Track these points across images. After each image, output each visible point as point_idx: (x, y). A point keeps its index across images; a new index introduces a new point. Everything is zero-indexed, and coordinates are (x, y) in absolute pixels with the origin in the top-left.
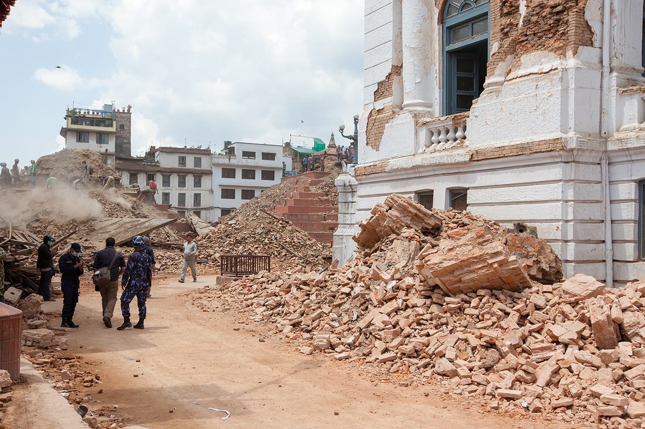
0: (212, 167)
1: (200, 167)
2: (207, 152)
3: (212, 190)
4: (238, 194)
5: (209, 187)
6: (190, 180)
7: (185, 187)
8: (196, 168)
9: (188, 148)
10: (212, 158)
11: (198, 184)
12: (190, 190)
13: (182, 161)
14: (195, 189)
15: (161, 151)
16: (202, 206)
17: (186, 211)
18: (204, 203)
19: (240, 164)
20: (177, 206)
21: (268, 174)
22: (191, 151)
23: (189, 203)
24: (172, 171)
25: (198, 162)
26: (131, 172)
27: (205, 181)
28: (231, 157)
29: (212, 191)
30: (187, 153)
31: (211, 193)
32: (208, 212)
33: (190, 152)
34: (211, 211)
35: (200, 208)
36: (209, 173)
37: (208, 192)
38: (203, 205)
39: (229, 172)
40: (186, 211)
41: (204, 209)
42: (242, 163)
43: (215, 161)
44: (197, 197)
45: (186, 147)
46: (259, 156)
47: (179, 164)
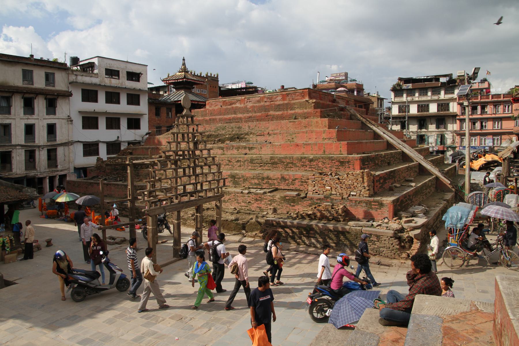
0: (68, 87)
1: (54, 86)
6: (40, 105)
9: (35, 57)
13: (27, 76)
14: (47, 117)
17: (37, 150)
18: (61, 136)
20: (23, 143)
22: (42, 63)
25: (49, 79)
30: (34, 65)
31: (70, 123)
32: (66, 148)
34: (71, 147)
37: (65, 121)
44: (51, 129)
45: (32, 56)
46: (123, 75)
47: (23, 81)
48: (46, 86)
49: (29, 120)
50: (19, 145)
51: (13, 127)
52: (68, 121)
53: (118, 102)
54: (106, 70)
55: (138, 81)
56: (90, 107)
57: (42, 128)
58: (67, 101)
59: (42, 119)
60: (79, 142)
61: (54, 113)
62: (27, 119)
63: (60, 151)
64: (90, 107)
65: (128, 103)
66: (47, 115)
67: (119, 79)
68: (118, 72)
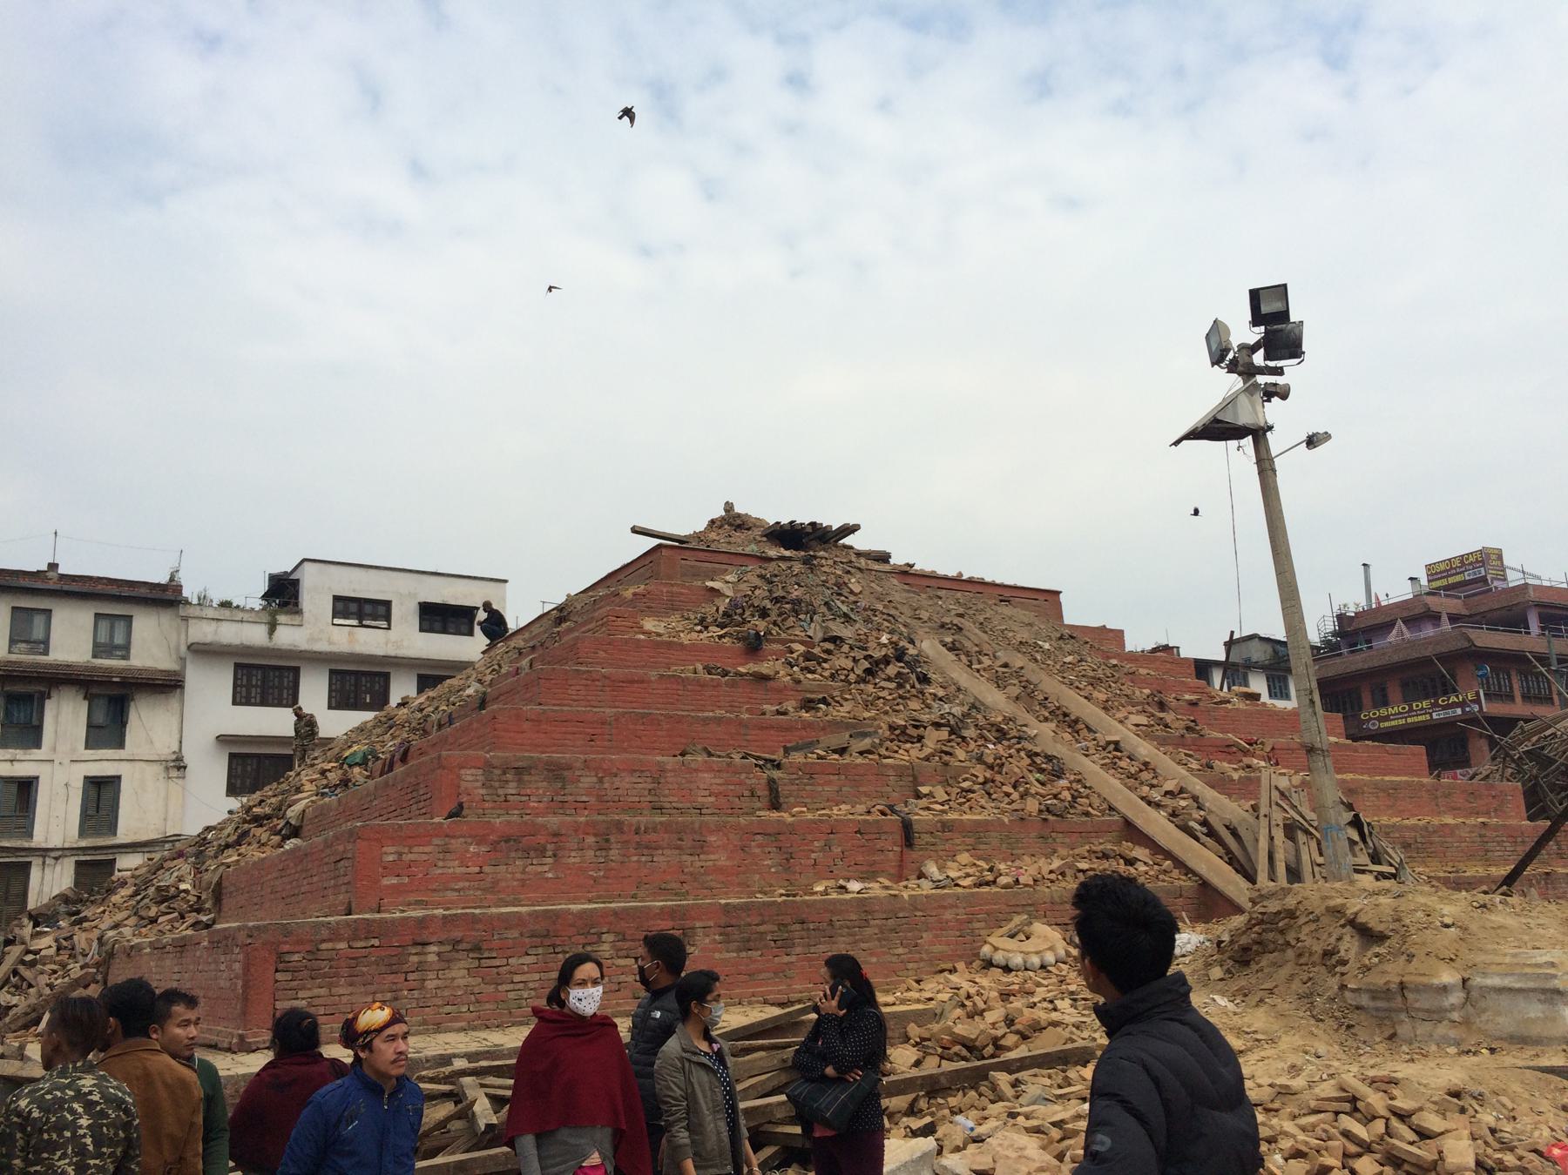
2: (164, 597)
3: (179, 759)
5: (164, 745)
7: (38, 745)
8: (99, 662)
9: (61, 570)
10: (185, 619)
14: (91, 754)
17: (36, 862)
19: (322, 646)
28: (282, 618)
29: (177, 765)
31: (174, 773)
33: (74, 587)
36: (167, 685)
40: (36, 862)
42: (330, 643)
43: (203, 632)
45: (53, 566)
47: (12, 642)
52: (167, 769)
54: (337, 599)
57: (62, 791)
58: (174, 703)
59: (66, 762)
61: (120, 744)
62: (12, 761)
67: (389, 628)
68: (388, 604)
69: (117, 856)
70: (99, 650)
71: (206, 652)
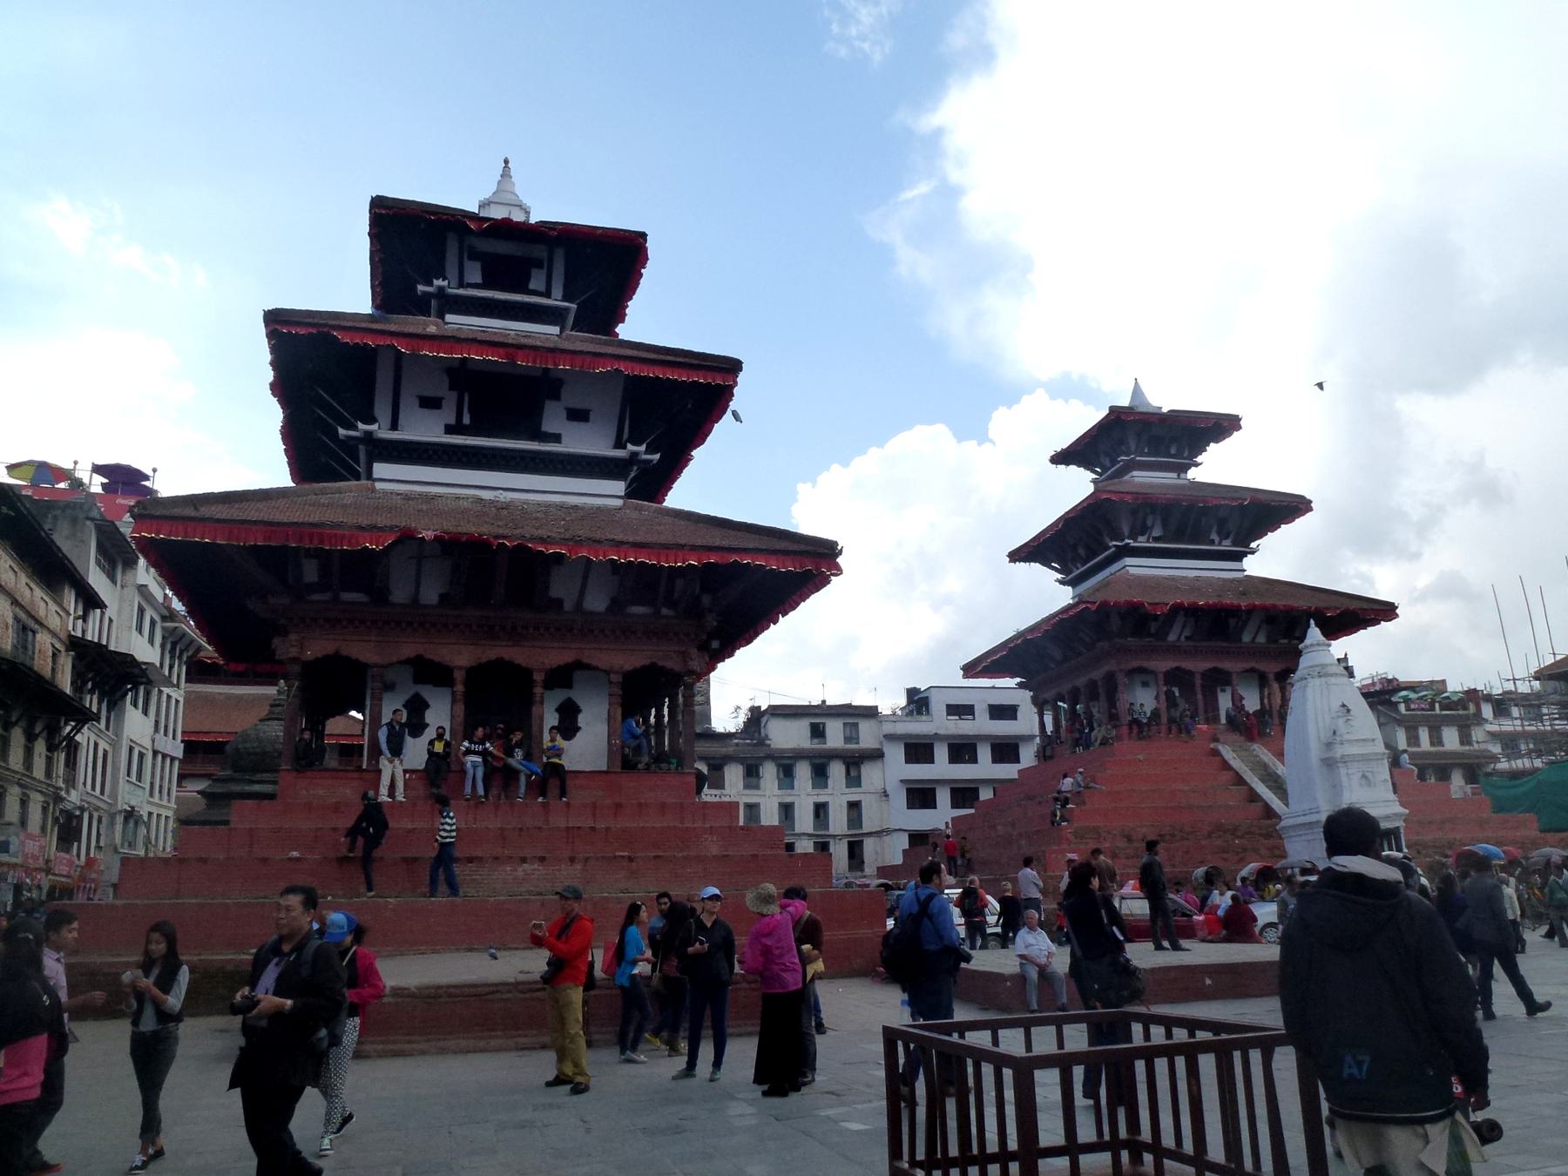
1: (858, 743)
2: (871, 712)
3: (885, 792)
4: (943, 797)
5: (879, 786)
6: (837, 770)
7: (826, 787)
9: (828, 703)
10: (881, 722)
11: (854, 781)
12: (837, 794)
13: (818, 732)
14: (847, 790)
15: (773, 715)
16: (865, 830)
20: (811, 830)
21: (1005, 750)
23: (838, 821)
24: (799, 755)
26: (712, 762)
27: (871, 774)
31: (884, 798)
34: (887, 839)
35: (861, 832)
36: (877, 755)
38: (868, 824)
39: (919, 751)
41: (870, 834)
43: (888, 728)
44: (854, 806)
45: (824, 702)
48: (845, 743)
49: (820, 797)
50: (804, 834)
51: (796, 806)
53: (974, 760)
54: (949, 706)
55: (1015, 718)
56: (920, 772)
57: (839, 808)
60: (900, 830)
63: (869, 846)
64: (920, 772)
65: (995, 761)
66: (847, 787)
67: (974, 719)
69: (865, 839)
70: (847, 740)
71: (890, 737)
